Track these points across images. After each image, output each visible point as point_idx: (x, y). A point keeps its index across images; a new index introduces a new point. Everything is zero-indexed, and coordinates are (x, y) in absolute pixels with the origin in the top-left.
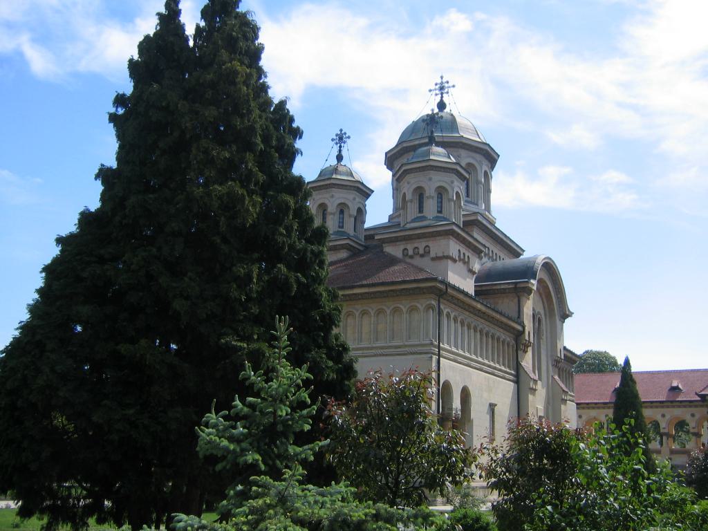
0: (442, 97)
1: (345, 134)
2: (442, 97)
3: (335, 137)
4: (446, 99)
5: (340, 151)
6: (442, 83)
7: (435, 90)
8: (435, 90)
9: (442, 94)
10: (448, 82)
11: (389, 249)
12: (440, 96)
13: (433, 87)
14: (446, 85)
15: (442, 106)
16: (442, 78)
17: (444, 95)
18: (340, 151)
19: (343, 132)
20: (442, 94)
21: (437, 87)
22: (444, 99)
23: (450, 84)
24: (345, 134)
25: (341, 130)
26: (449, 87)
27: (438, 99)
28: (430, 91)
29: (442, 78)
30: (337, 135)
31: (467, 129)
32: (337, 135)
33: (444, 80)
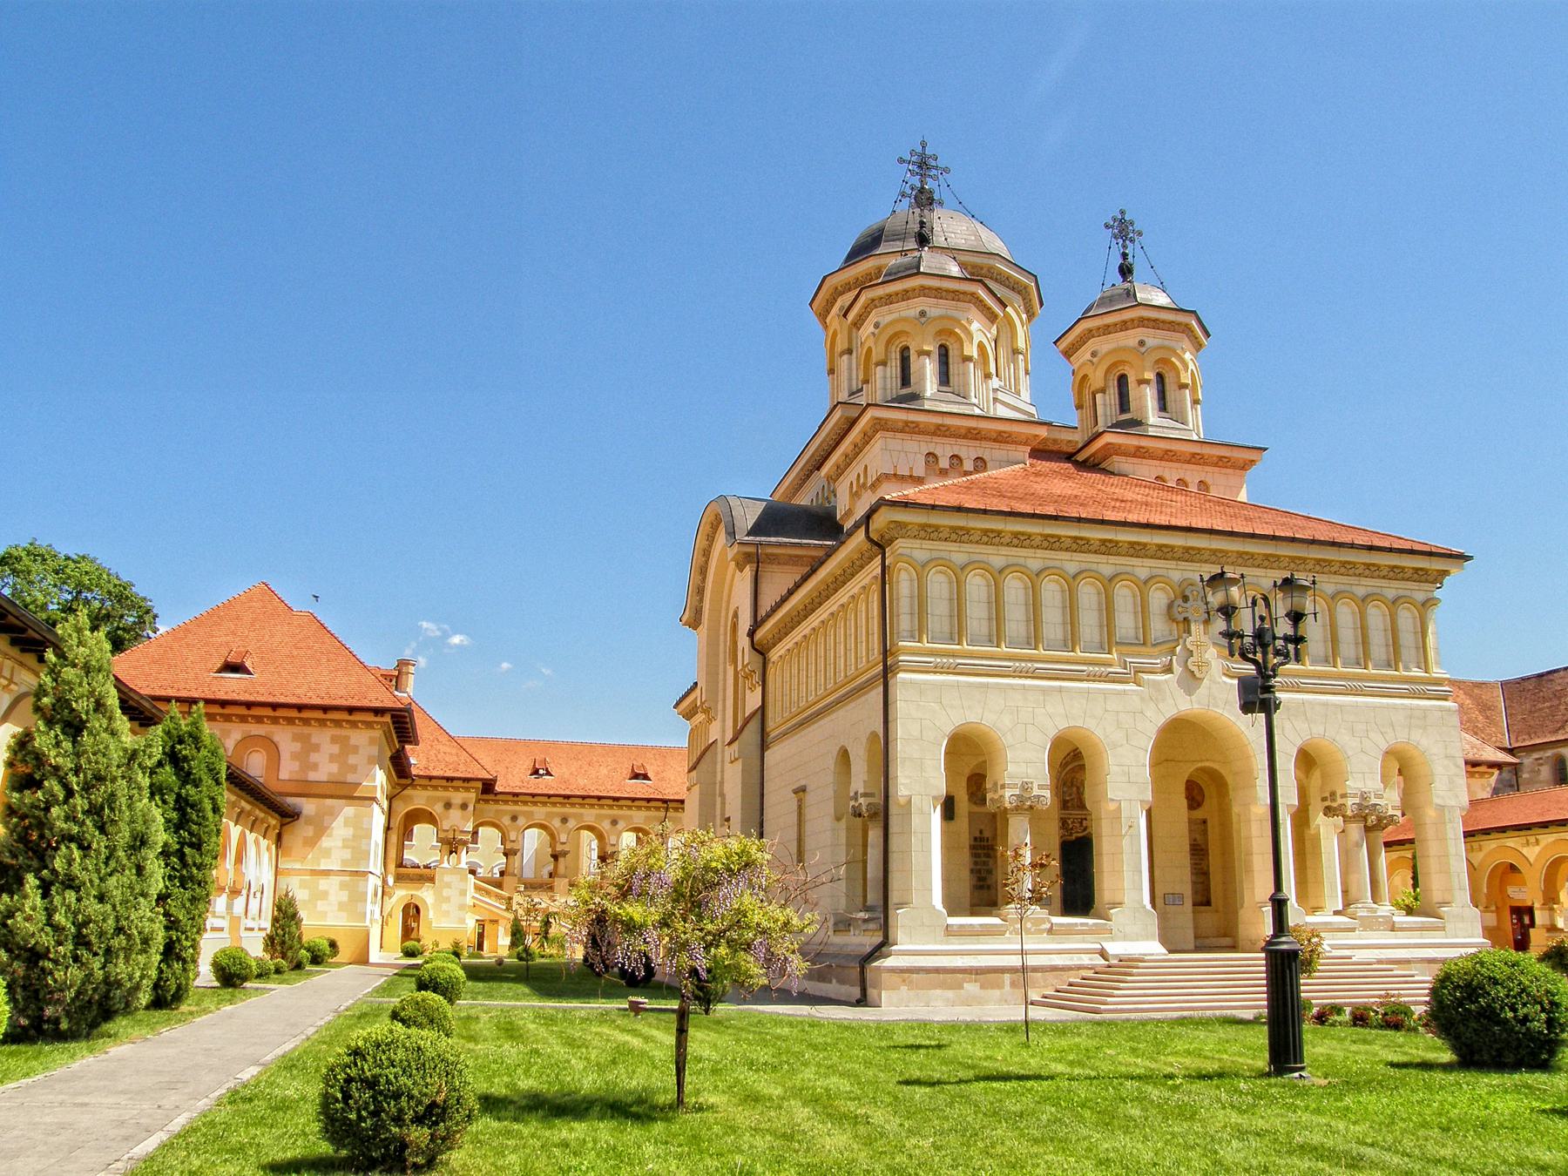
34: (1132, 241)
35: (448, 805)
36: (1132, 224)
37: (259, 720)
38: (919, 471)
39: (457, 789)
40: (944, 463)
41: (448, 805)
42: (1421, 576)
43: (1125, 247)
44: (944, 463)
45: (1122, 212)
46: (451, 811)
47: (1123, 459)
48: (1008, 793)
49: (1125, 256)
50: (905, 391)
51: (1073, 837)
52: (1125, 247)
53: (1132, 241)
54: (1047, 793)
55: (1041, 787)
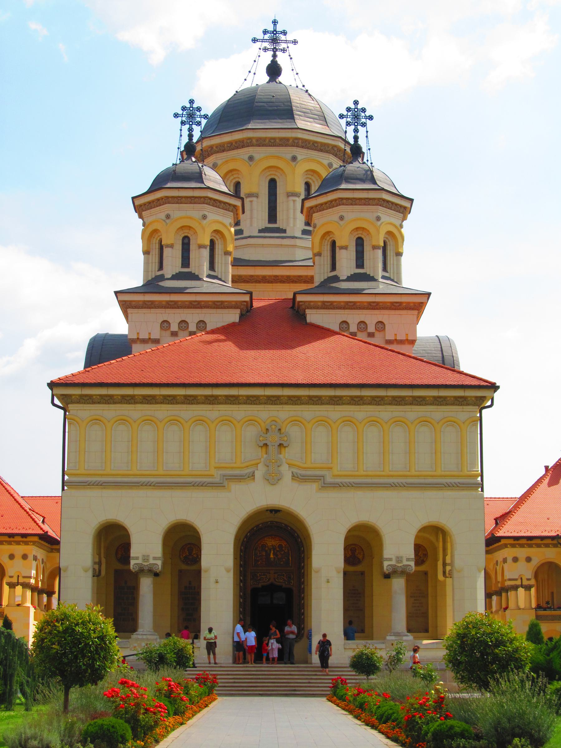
0: (275, 56)
1: (199, 109)
2: (275, 56)
3: (180, 112)
4: (281, 59)
5: (191, 136)
6: (275, 32)
7: (263, 41)
9: (275, 50)
10: (284, 33)
11: (313, 317)
12: (272, 53)
13: (260, 36)
14: (283, 37)
16: (275, 22)
17: (277, 53)
18: (191, 136)
19: (195, 106)
20: (275, 50)
21: (267, 37)
22: (277, 59)
23: (289, 37)
26: (286, 42)
27: (267, 58)
28: (255, 40)
29: (275, 22)
30: (184, 108)
31: (307, 113)
32: (184, 108)
33: (279, 28)
34: (364, 125)
35: (12, 557)
36: (364, 110)
38: (156, 334)
39: (18, 543)
40: (174, 327)
41: (12, 557)
42: (461, 401)
43: (356, 131)
44: (174, 327)
47: (314, 311)
48: (132, 562)
49: (356, 138)
50: (160, 273)
51: (260, 586)
52: (356, 131)
53: (364, 125)
54: (159, 563)
55: (155, 558)
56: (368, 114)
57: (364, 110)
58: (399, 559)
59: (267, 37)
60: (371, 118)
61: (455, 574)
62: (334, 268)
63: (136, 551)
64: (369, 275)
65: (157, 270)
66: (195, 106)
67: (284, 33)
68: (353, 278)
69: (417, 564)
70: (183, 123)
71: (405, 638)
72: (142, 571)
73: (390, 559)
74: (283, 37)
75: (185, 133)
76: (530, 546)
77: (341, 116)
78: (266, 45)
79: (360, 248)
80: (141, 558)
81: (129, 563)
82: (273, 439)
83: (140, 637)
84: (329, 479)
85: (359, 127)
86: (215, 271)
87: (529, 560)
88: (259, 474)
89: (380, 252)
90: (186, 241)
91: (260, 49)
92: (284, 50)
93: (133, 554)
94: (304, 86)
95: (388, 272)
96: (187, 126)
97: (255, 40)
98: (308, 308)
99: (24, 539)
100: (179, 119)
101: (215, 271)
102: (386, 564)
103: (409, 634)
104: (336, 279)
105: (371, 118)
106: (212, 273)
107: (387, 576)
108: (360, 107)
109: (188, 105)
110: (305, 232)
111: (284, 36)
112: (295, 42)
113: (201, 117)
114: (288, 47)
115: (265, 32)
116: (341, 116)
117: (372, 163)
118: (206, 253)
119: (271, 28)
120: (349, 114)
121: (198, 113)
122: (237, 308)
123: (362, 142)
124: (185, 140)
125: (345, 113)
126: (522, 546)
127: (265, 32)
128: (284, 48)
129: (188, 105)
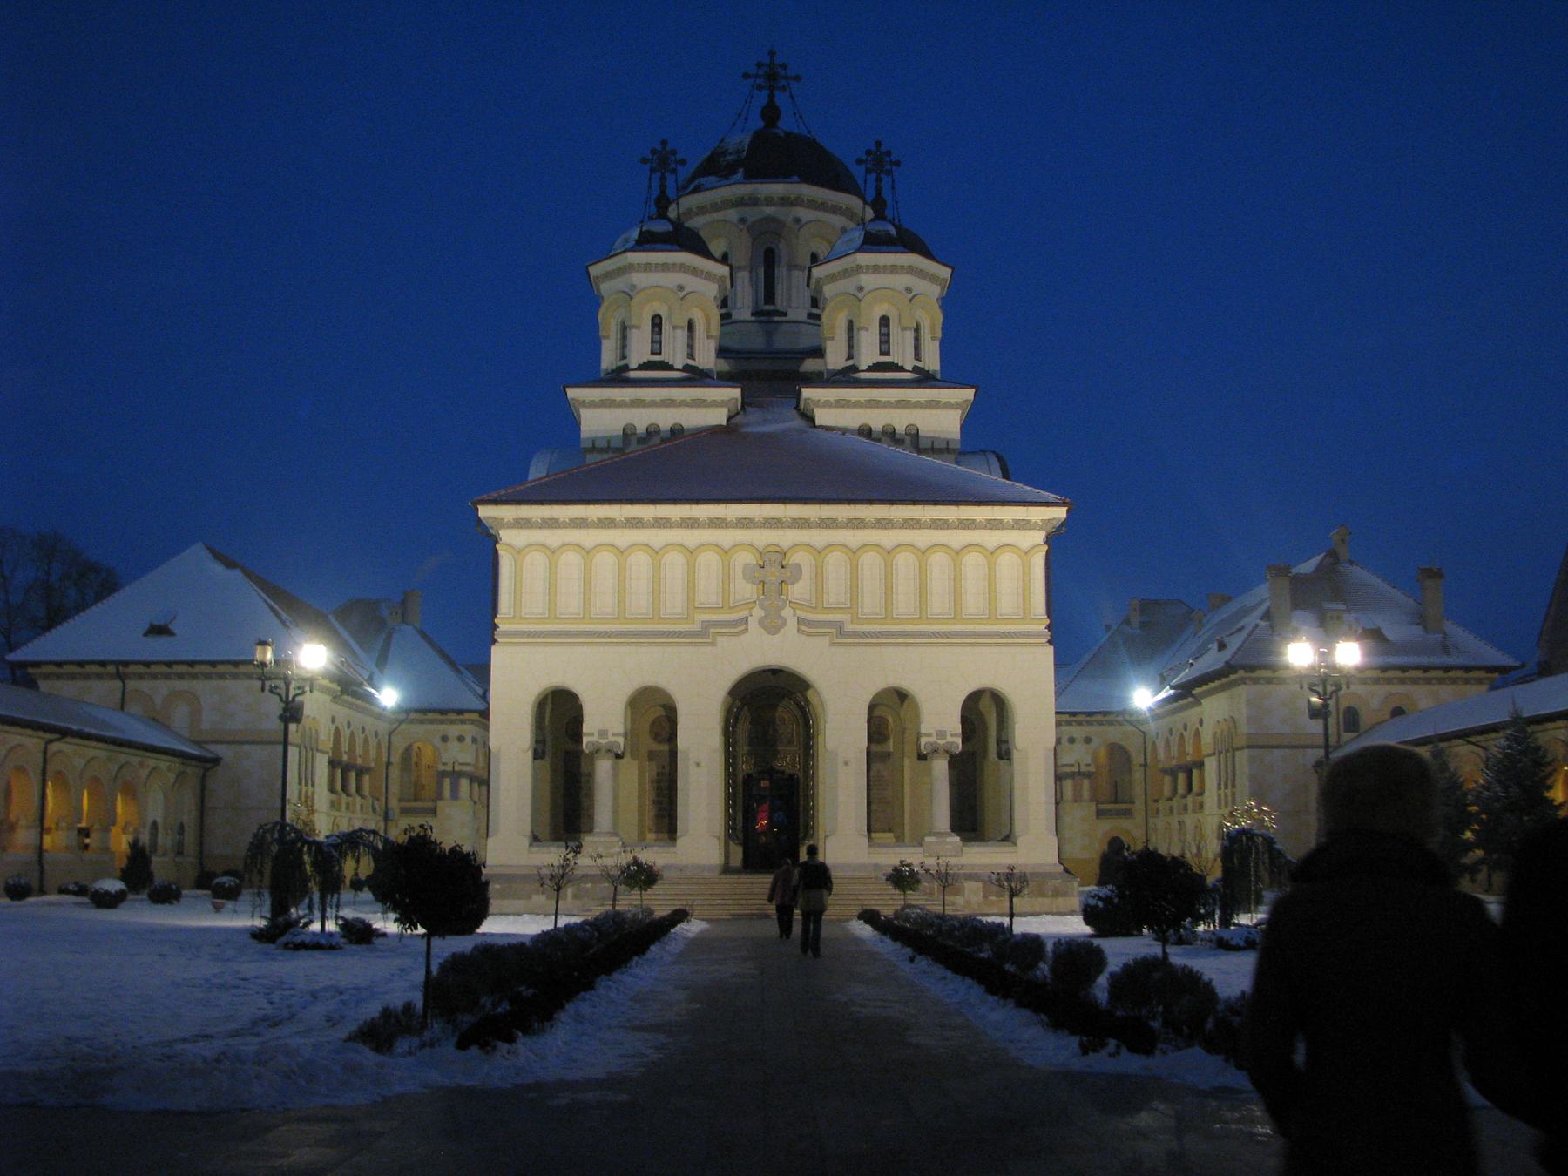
0: (771, 96)
1: (674, 152)
2: (771, 96)
4: (781, 99)
7: (757, 76)
8: (757, 76)
9: (772, 89)
14: (782, 73)
15: (771, 113)
16: (772, 54)
19: (668, 148)
20: (772, 89)
21: (761, 72)
24: (674, 152)
25: (664, 143)
26: (786, 78)
27: (762, 98)
28: (746, 76)
29: (772, 54)
30: (653, 152)
32: (653, 152)
34: (889, 172)
35: (445, 739)
36: (889, 153)
37: (181, 676)
43: (879, 180)
45: (879, 144)
46: (449, 744)
48: (585, 740)
52: (879, 180)
53: (889, 172)
54: (621, 740)
56: (893, 158)
57: (889, 153)
58: (941, 734)
59: (761, 72)
60: (898, 163)
61: (1016, 755)
62: (850, 357)
63: (589, 727)
64: (897, 364)
65: (618, 358)
66: (668, 148)
67: (784, 67)
68: (877, 367)
69: (963, 742)
70: (652, 171)
71: (949, 839)
72: (597, 750)
73: (929, 735)
74: (782, 73)
75: (656, 183)
76: (1089, 723)
77: (859, 162)
78: (759, 81)
79: (884, 330)
80: (596, 734)
81: (580, 741)
82: (773, 575)
83: (596, 839)
84: (849, 627)
85: (883, 176)
86: (694, 359)
87: (1088, 740)
88: (753, 623)
89: (910, 335)
90: (657, 321)
91: (753, 86)
92: (784, 89)
93: (585, 729)
94: (809, 132)
95: (921, 361)
96: (659, 174)
97: (746, 76)
98: (818, 406)
99: (460, 717)
100: (648, 166)
101: (694, 359)
102: (923, 740)
103: (953, 834)
104: (855, 369)
105: (898, 163)
106: (691, 362)
107: (922, 757)
108: (883, 149)
109: (659, 148)
110: (810, 316)
111: (784, 72)
112: (797, 78)
113: (677, 162)
114: (789, 85)
115: (759, 65)
116: (859, 162)
117: (899, 220)
118: (682, 335)
119: (767, 60)
120: (869, 158)
121: (673, 158)
122: (725, 406)
123: (886, 194)
124: (656, 192)
125: (864, 157)
126: (1080, 723)
127: (759, 65)
128: (784, 86)
129: (659, 148)
